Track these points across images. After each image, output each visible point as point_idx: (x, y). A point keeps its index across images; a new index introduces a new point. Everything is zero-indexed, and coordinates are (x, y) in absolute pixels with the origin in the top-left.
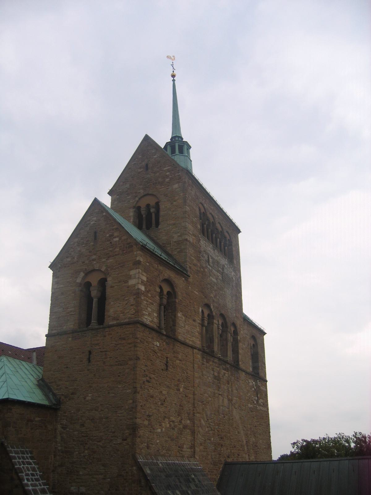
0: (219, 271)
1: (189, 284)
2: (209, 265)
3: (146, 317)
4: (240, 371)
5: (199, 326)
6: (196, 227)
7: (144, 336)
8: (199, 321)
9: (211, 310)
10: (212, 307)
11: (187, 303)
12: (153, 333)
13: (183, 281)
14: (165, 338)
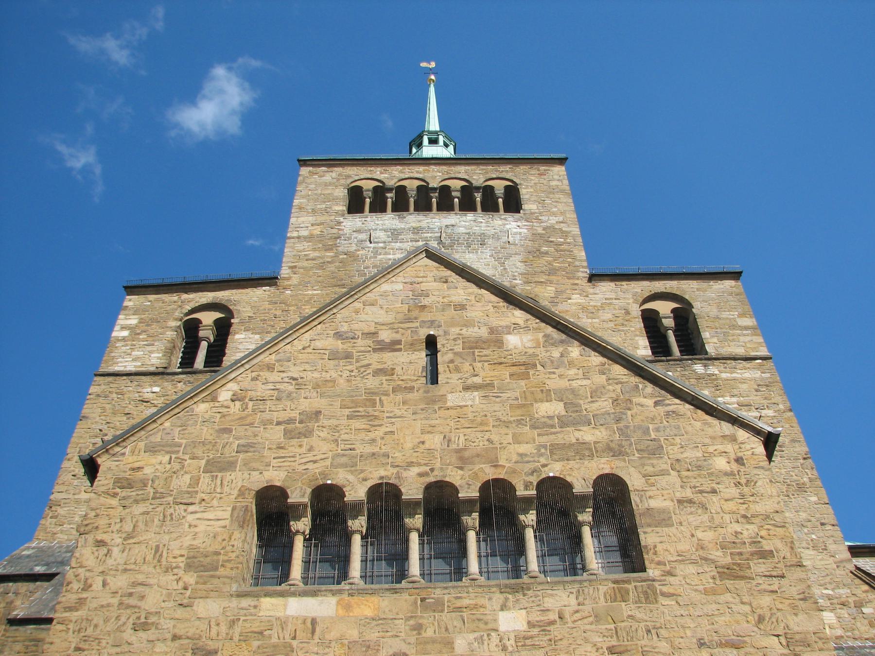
0: (427, 237)
11: (276, 315)
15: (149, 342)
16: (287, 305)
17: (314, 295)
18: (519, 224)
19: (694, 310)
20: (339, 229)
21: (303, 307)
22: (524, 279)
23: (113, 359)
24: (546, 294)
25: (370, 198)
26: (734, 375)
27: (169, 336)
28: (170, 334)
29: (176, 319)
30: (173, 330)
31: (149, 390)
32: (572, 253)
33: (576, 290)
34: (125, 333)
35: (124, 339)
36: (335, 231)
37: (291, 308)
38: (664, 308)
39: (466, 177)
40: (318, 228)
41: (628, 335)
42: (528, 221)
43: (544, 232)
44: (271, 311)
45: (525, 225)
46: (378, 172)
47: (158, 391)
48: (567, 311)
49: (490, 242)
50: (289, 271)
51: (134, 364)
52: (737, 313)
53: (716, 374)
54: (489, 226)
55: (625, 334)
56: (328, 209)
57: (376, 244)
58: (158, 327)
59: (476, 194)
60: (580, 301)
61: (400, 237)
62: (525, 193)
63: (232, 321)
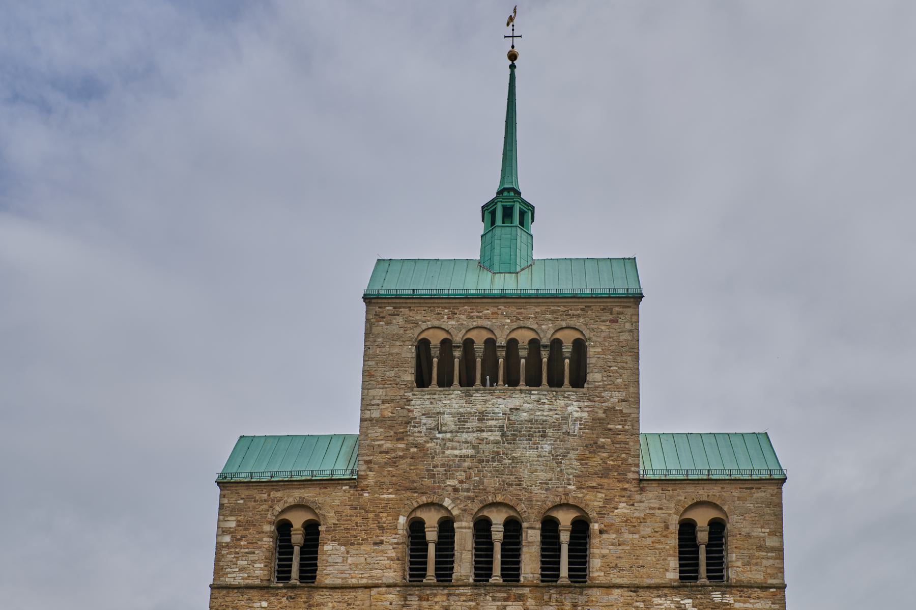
0: (491, 426)
1: (362, 490)
2: (440, 433)
3: (234, 575)
4: (596, 593)
5: (393, 548)
6: (397, 384)
7: (227, 601)
8: (396, 541)
9: (446, 509)
10: (447, 503)
11: (357, 523)
12: (251, 592)
13: (344, 491)
14: (285, 591)
15: (250, 550)
16: (367, 512)
17: (389, 500)
18: (581, 404)
19: (728, 526)
20: (409, 411)
21: (381, 515)
22: (578, 484)
23: (222, 569)
24: (596, 504)
25: (437, 357)
26: (748, 605)
27: (266, 543)
28: (267, 542)
29: (270, 523)
30: (269, 536)
31: (259, 604)
32: (627, 446)
33: (624, 497)
34: (227, 539)
35: (228, 546)
36: (405, 412)
37: (371, 515)
38: (702, 518)
39: (535, 327)
40: (388, 408)
41: (662, 554)
42: (590, 401)
43: (603, 416)
44: (354, 517)
45: (587, 406)
46: (446, 316)
47: (266, 606)
48: (612, 525)
49: (550, 432)
50: (364, 467)
51: (241, 575)
52: (768, 530)
53: (731, 604)
54: (551, 410)
55: (660, 553)
56: (398, 379)
57: (444, 434)
58: (255, 532)
59: (543, 353)
60: (626, 511)
61: (467, 425)
62: (591, 352)
63: (320, 528)
